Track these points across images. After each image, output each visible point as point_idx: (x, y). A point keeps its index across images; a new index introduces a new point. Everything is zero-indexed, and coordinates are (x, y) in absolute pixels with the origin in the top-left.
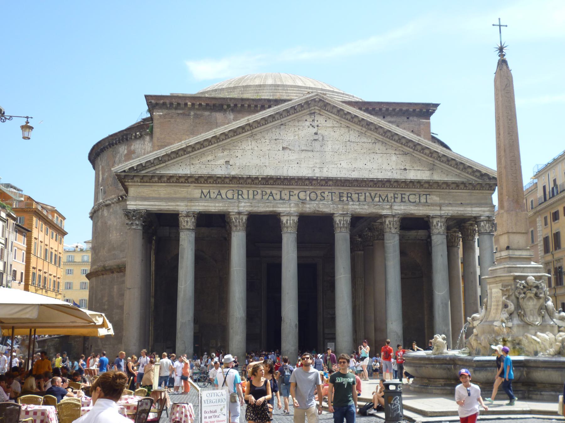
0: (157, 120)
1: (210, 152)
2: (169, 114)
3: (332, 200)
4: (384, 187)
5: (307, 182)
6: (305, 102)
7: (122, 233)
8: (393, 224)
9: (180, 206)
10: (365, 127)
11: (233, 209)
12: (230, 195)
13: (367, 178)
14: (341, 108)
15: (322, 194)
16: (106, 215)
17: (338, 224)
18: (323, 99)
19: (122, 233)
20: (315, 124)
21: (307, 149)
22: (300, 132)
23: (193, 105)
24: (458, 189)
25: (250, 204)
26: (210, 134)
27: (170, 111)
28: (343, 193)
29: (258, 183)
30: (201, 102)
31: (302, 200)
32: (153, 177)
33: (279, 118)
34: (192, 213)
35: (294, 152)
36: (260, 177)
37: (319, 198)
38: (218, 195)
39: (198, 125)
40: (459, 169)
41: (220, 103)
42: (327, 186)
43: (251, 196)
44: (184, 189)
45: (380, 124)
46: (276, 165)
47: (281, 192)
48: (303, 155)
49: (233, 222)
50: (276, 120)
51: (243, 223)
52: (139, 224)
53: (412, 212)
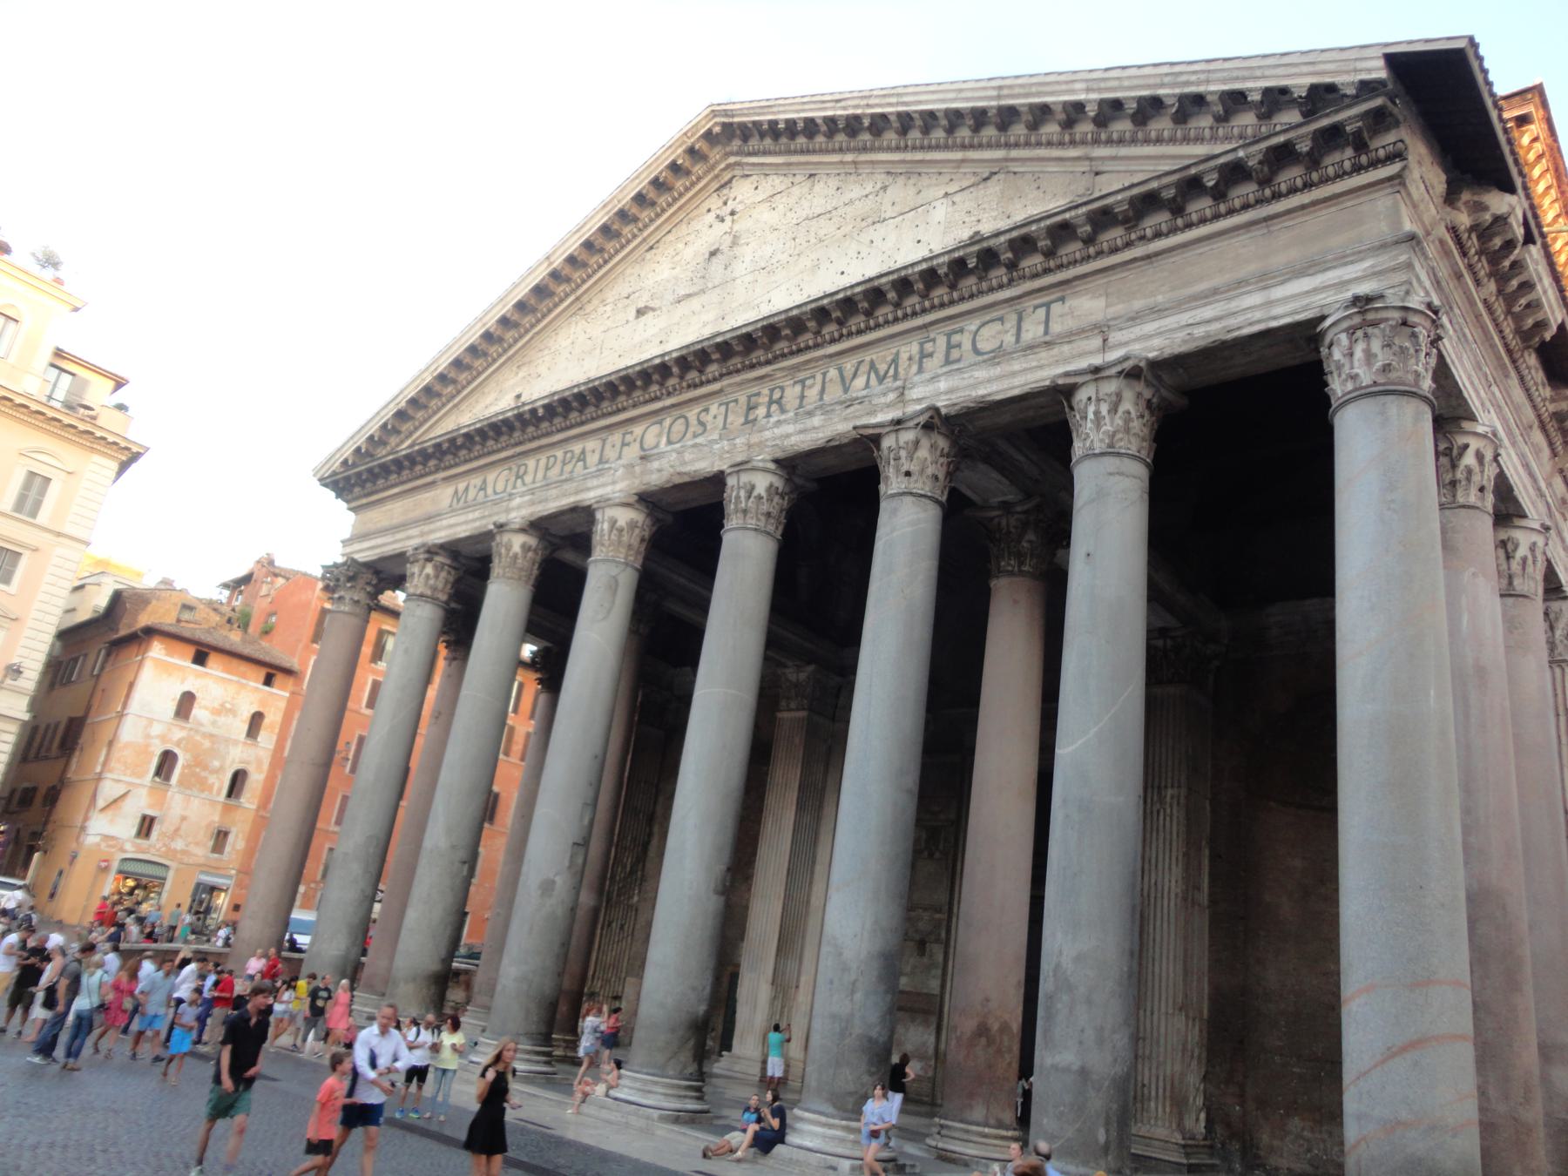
3: (724, 427)
4: (878, 326)
6: (691, 151)
10: (849, 150)
15: (703, 414)
24: (1189, 226)
28: (758, 394)
32: (373, 475)
33: (635, 230)
37: (691, 430)
38: (481, 489)
40: (1199, 139)
42: (709, 382)
43: (540, 475)
48: (683, 308)
50: (628, 242)
51: (515, 556)
52: (340, 598)
53: (981, 392)
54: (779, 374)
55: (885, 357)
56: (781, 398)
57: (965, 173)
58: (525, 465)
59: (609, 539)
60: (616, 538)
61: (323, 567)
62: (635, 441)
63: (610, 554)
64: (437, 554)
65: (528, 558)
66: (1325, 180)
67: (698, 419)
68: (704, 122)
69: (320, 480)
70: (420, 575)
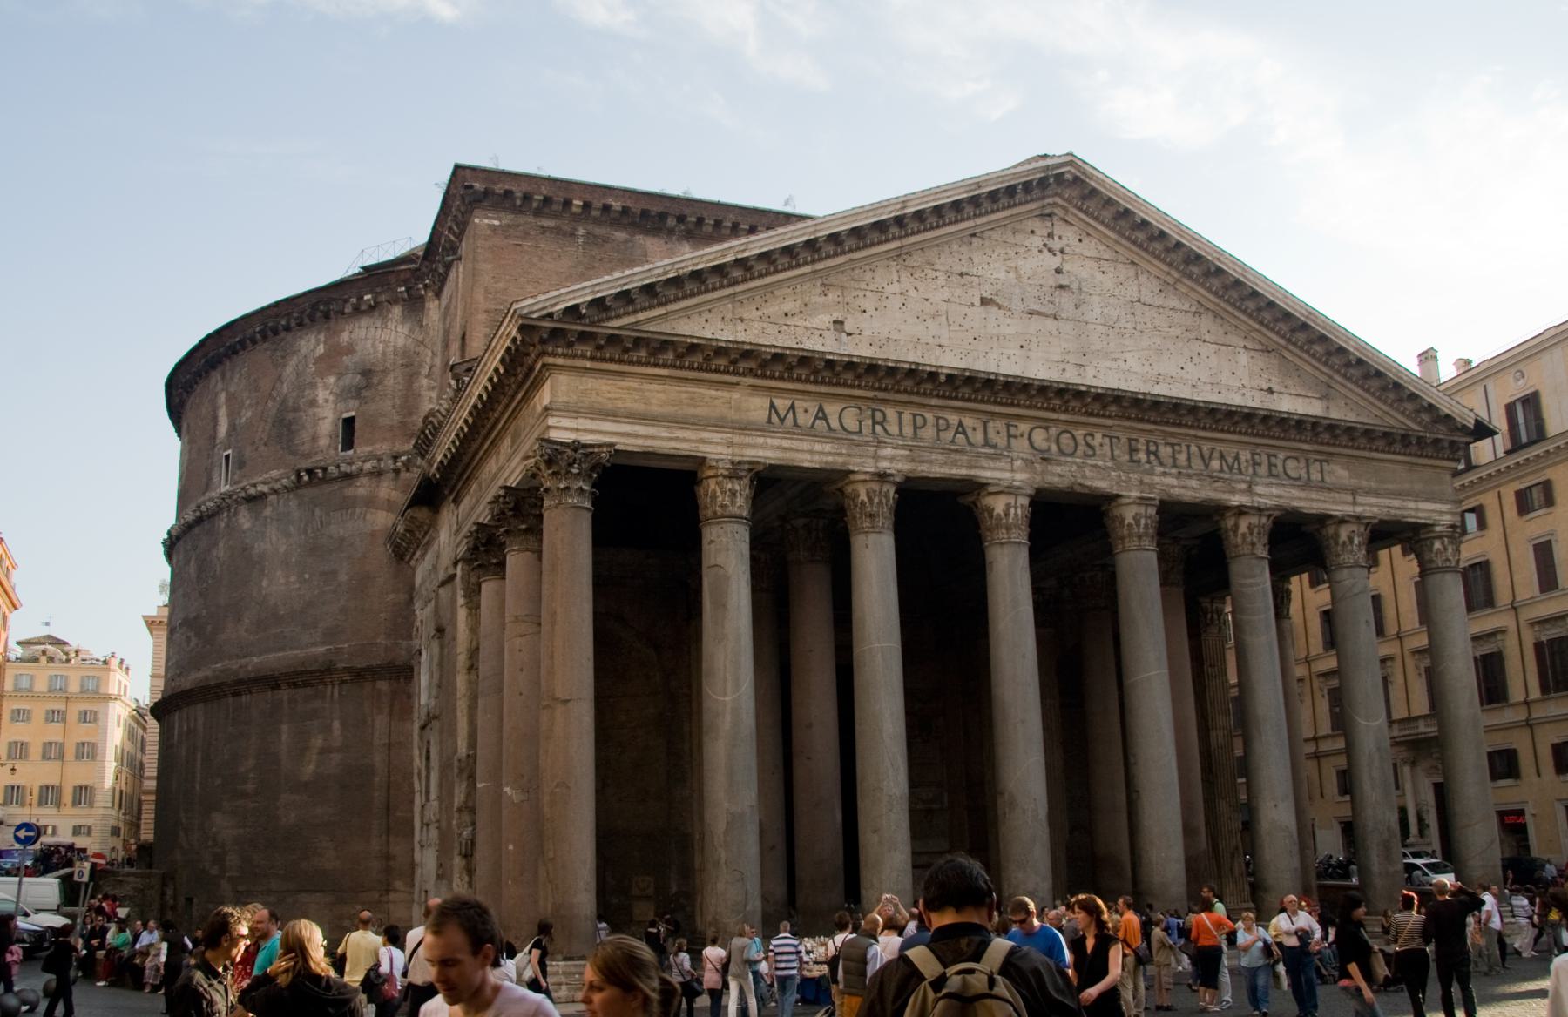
0: (486, 240)
1: (790, 290)
2: (518, 226)
3: (1113, 457)
4: (1234, 432)
5: (1057, 402)
6: (1041, 179)
7: (307, 576)
8: (1259, 533)
9: (711, 443)
10: (1177, 269)
11: (863, 464)
12: (850, 422)
13: (1204, 402)
15: (1089, 438)
16: (247, 525)
17: (1130, 525)
18: (1083, 177)
19: (307, 576)
20: (1056, 244)
21: (1042, 310)
22: (1021, 262)
23: (587, 206)
24: (1389, 452)
25: (907, 453)
26: (802, 232)
27: (522, 219)
28: (1137, 440)
30: (610, 201)
31: (1041, 451)
34: (746, 466)
35: (1010, 313)
36: (945, 371)
38: (817, 417)
39: (597, 265)
40: (1385, 402)
41: (660, 209)
42: (1104, 416)
43: (908, 430)
44: (719, 393)
46: (968, 347)
47: (985, 424)
49: (862, 501)
50: (963, 220)
53: (1296, 504)
58: (884, 415)
66: (1437, 458)
67: (1085, 440)
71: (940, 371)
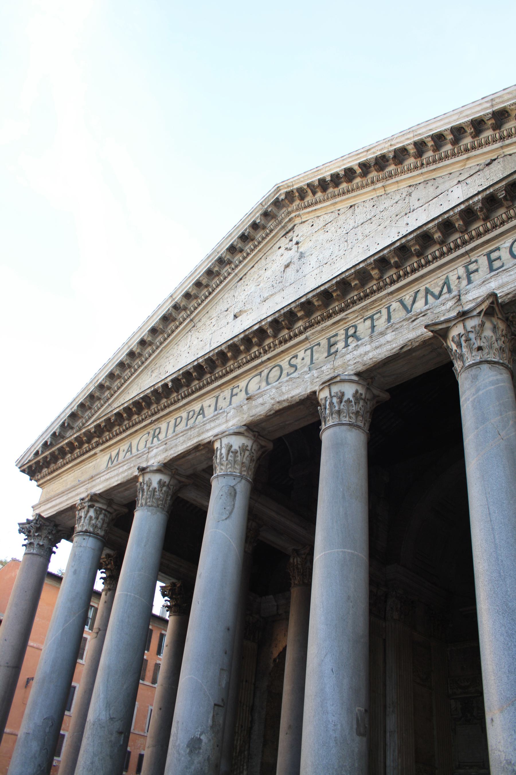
4: (428, 263)
8: (468, 340)
14: (319, 177)
15: (293, 361)
21: (273, 292)
28: (336, 335)
29: (177, 396)
33: (229, 270)
34: (87, 499)
35: (251, 311)
37: (285, 372)
42: (296, 336)
43: (171, 431)
45: (394, 145)
50: (225, 278)
51: (154, 490)
54: (351, 317)
55: (436, 283)
56: (355, 332)
57: (470, 167)
58: (160, 428)
59: (227, 459)
60: (232, 459)
61: (19, 524)
62: (241, 391)
63: (228, 471)
64: (97, 501)
65: (163, 491)
68: (273, 195)
69: (20, 468)
70: (85, 517)
71: (166, 381)
